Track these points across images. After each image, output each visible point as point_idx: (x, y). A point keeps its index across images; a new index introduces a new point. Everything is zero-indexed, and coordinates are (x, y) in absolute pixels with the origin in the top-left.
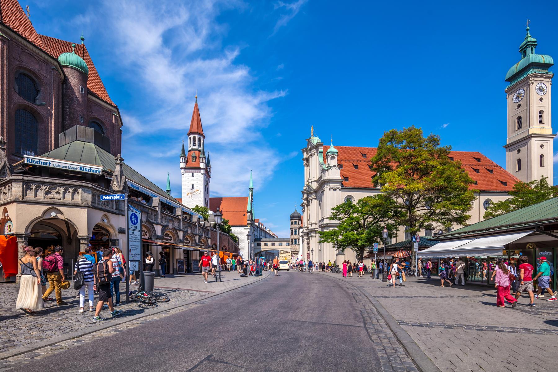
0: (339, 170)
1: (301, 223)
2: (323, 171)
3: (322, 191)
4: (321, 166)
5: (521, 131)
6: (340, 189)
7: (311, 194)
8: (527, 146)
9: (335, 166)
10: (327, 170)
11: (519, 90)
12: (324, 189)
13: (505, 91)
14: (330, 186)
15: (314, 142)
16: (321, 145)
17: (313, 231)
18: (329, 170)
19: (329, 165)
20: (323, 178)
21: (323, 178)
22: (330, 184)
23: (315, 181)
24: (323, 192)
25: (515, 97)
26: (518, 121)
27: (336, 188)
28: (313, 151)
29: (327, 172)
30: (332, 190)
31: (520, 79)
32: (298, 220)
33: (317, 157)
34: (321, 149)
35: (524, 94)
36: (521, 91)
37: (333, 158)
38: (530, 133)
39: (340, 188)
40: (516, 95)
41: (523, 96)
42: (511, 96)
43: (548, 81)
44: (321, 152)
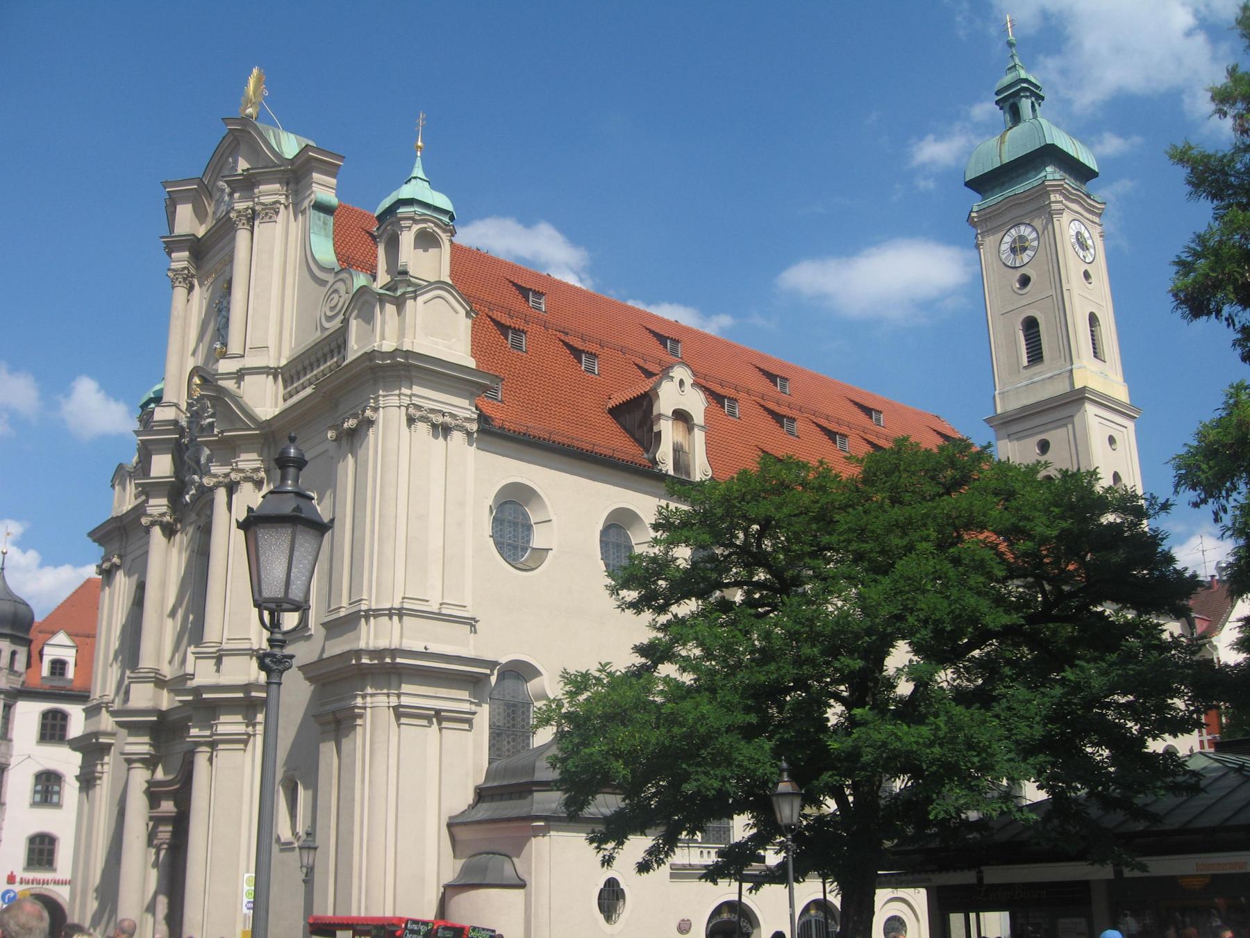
0: (468, 315)
1: (29, 665)
2: (364, 303)
3: (351, 423)
4: (323, 283)
5: (1042, 371)
6: (469, 434)
7: (228, 449)
8: (1070, 426)
9: (440, 285)
10: (400, 303)
11: (1018, 225)
12: (368, 413)
13: (969, 218)
14: (416, 400)
15: (279, 144)
16: (331, 170)
17: (230, 706)
18: (410, 303)
19: (405, 273)
20: (355, 348)
21: (355, 348)
22: (417, 390)
23: (265, 371)
24: (353, 438)
25: (1008, 246)
26: (1025, 336)
27: (448, 419)
28: (270, 192)
29: (390, 309)
30: (422, 428)
31: (1020, 188)
32: (15, 639)
33: (295, 228)
34: (323, 189)
35: (1035, 243)
36: (1025, 231)
37: (426, 240)
38: (1078, 385)
39: (474, 427)
40: (1007, 239)
41: (1036, 250)
42: (990, 241)
43: (1095, 223)
44: (321, 207)
